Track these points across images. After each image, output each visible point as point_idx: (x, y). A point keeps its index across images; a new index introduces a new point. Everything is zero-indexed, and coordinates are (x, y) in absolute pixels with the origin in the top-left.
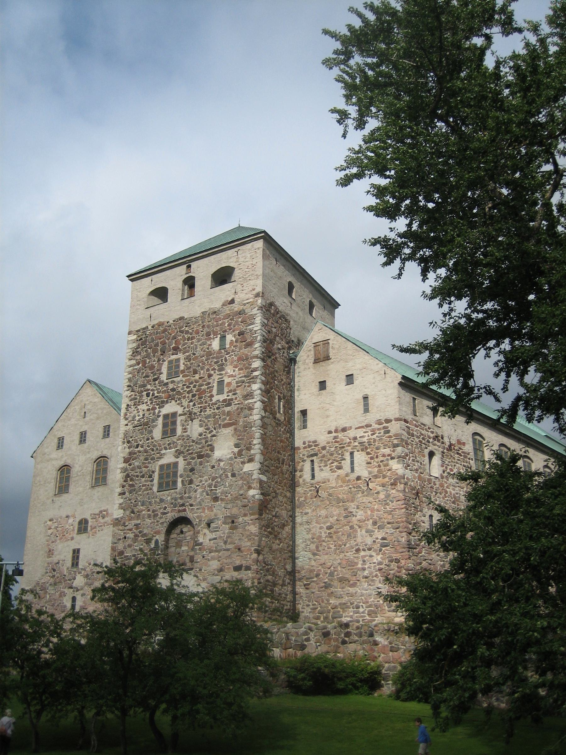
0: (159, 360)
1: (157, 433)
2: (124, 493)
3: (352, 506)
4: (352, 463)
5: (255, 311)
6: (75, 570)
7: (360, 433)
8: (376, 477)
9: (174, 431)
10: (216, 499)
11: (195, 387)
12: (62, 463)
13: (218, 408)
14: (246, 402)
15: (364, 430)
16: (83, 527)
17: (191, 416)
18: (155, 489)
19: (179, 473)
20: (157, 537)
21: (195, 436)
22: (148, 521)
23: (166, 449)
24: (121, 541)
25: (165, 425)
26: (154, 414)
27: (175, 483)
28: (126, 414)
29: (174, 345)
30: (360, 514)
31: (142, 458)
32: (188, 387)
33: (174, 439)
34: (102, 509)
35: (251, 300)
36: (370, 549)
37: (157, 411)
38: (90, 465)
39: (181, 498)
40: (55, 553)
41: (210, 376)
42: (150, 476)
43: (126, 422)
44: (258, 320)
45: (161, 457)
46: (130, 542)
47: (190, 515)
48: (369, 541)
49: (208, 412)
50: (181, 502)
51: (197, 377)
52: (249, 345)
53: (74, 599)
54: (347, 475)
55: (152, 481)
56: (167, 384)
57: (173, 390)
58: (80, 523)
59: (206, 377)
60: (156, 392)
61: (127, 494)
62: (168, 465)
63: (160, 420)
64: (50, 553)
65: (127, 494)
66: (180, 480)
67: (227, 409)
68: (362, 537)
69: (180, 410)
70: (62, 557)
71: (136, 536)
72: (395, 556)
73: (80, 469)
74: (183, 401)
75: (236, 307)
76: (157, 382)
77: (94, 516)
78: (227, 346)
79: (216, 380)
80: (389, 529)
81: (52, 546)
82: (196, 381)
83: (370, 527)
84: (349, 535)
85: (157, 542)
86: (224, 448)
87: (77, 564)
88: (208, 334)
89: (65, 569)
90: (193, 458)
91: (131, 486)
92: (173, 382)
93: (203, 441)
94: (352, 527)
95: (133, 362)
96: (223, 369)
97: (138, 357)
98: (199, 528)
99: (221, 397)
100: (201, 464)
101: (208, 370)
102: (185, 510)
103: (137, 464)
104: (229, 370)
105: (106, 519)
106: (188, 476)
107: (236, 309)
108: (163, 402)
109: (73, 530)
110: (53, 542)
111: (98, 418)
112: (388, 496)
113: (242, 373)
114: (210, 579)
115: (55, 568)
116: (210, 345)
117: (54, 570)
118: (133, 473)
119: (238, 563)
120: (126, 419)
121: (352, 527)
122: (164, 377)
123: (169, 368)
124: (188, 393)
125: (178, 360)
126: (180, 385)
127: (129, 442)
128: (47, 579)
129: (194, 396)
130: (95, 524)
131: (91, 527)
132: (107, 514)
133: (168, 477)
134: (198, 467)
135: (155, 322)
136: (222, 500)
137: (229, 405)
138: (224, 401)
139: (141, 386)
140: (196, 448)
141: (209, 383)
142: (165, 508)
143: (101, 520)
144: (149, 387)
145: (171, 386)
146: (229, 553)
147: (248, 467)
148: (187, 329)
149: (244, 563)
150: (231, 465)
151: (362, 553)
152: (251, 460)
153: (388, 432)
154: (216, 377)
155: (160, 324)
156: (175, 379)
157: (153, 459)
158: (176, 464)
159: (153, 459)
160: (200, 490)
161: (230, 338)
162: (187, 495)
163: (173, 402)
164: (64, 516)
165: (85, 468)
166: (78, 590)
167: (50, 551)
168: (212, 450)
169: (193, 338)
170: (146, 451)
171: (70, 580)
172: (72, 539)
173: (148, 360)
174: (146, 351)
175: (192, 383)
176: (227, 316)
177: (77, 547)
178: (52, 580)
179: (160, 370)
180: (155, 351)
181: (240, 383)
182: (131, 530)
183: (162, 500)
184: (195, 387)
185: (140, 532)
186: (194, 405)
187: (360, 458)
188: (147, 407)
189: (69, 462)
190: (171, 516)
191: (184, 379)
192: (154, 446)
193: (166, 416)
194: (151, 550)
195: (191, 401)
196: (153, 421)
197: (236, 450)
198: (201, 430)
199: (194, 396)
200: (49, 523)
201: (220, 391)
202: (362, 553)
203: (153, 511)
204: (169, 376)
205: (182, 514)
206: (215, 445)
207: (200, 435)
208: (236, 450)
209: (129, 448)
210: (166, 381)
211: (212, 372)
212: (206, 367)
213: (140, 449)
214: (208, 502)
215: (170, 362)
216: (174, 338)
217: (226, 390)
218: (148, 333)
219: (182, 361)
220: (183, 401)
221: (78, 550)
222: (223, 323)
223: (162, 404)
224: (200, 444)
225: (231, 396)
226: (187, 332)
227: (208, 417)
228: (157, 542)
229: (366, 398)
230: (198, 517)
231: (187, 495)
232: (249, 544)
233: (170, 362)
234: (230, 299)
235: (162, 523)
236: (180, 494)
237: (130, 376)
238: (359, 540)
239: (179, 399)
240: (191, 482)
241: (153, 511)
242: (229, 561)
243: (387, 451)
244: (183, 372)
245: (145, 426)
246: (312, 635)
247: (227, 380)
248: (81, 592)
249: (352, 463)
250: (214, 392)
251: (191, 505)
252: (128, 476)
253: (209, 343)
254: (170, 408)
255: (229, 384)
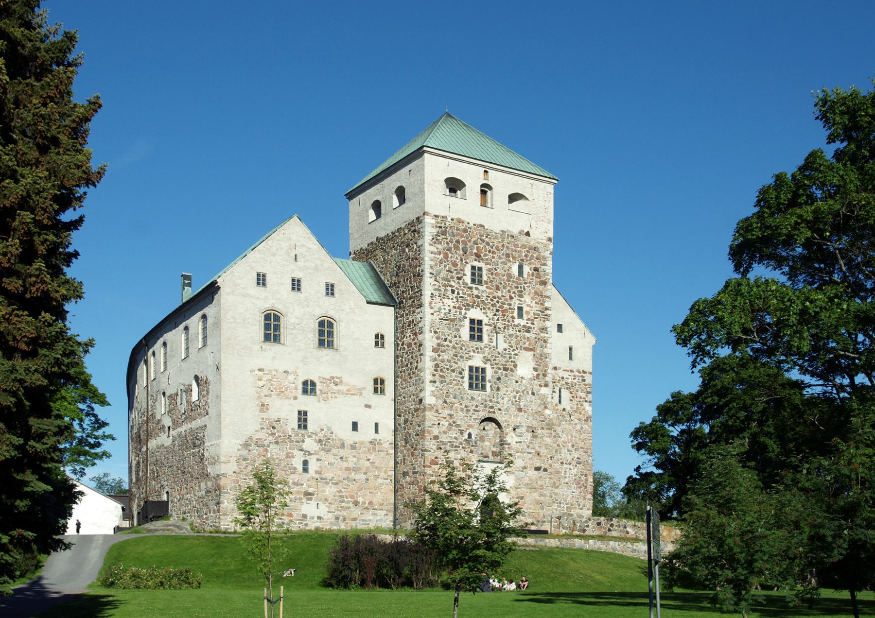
0: (461, 260)
1: (465, 332)
2: (435, 382)
3: (559, 430)
4: (560, 397)
5: (547, 254)
6: (303, 432)
7: (566, 375)
8: (575, 411)
9: (480, 339)
10: (520, 410)
11: (498, 302)
12: (268, 305)
13: (519, 331)
14: (542, 335)
15: (570, 373)
16: (309, 388)
17: (496, 330)
18: (466, 385)
19: (487, 379)
20: (471, 430)
21: (500, 349)
22: (461, 414)
23: (474, 352)
24: (436, 426)
25: (472, 329)
26: (460, 313)
27: (484, 388)
28: (431, 303)
29: (475, 251)
30: (564, 438)
31: (452, 353)
32: (491, 300)
33: (482, 345)
34: (334, 375)
35: (544, 242)
36: (570, 464)
37: (463, 311)
38: (312, 321)
39: (491, 401)
40: (271, 409)
41: (511, 298)
42: (461, 373)
43: (432, 311)
44: (550, 263)
45: (469, 358)
46: (444, 429)
47: (499, 419)
48: (569, 458)
49: (511, 331)
50: (491, 404)
51: (499, 294)
52: (544, 283)
53: (305, 463)
54: (556, 405)
55: (463, 378)
56: (471, 288)
57: (478, 297)
58: (305, 383)
59: (508, 297)
60: (461, 292)
61: (438, 383)
62: (477, 369)
63: (467, 323)
64: (264, 407)
65: (438, 383)
66: (488, 385)
67: (527, 335)
68: (565, 455)
69: (485, 321)
70: (282, 416)
71: (450, 424)
72: (585, 472)
73: (297, 321)
74: (489, 312)
75: (532, 241)
76: (461, 282)
77: (324, 380)
78: (525, 276)
79: (517, 305)
80: (581, 451)
81: (266, 400)
82: (499, 298)
83: (570, 448)
84: (556, 451)
85: (470, 435)
86: (525, 368)
87: (305, 427)
88: (508, 255)
89: (290, 430)
90: (500, 369)
91: (440, 376)
92: (477, 289)
93: (508, 356)
94: (558, 445)
95: (434, 249)
96: (521, 296)
97: (439, 246)
98: (507, 430)
99: (523, 322)
100: (506, 376)
101: (509, 291)
102: (494, 412)
103: (446, 357)
104: (527, 299)
105: (340, 387)
106: (495, 383)
107: (532, 243)
108: (468, 305)
109: (296, 389)
110: (266, 396)
111: (316, 269)
112: (582, 428)
113: (539, 307)
114: (517, 473)
115: (275, 424)
116: (510, 268)
117: (274, 428)
118: (442, 364)
119: (538, 465)
120: (432, 308)
121: (558, 445)
122: (468, 279)
123: (473, 274)
124: (493, 305)
125: (480, 269)
126: (485, 295)
127: (436, 332)
128: (262, 435)
129: (497, 311)
130: (325, 389)
131: (321, 390)
132: (341, 382)
133: (477, 378)
134: (503, 378)
135: (455, 217)
136: (525, 412)
137: (528, 331)
138: (524, 326)
139: (443, 279)
140: (502, 361)
141: (510, 305)
142: (477, 406)
143: (332, 385)
144: (453, 283)
145: (475, 292)
146: (530, 456)
147: (544, 391)
148: (487, 240)
149: (543, 466)
150: (531, 385)
151: (565, 466)
152: (546, 385)
153: (584, 380)
154: (515, 303)
155: (460, 221)
156: (479, 287)
157: (462, 357)
158: (484, 370)
159: (462, 357)
160: (506, 399)
161: (526, 269)
162: (495, 400)
163: (479, 309)
164: (281, 370)
165: (305, 322)
166: (310, 454)
167: (263, 405)
168: (515, 366)
169: (493, 253)
170: (455, 348)
171: (298, 442)
172: (295, 398)
173: (450, 255)
174: (447, 243)
175: (495, 297)
176: (524, 246)
177: (303, 408)
178: (271, 438)
179: (462, 270)
180: (457, 248)
181: (536, 316)
182: (445, 418)
183: (473, 398)
184: (498, 302)
185: (454, 422)
186: (498, 320)
187: (565, 394)
188: (453, 305)
189: (279, 307)
190: (483, 414)
191: (488, 291)
192: (463, 345)
193: (472, 321)
194: (466, 440)
195: (495, 315)
196: (460, 320)
197: (535, 373)
198: (506, 346)
199: (497, 311)
200: (257, 372)
201: (520, 316)
202: (565, 466)
203: (466, 406)
204: (473, 281)
205: (492, 416)
206: (517, 363)
207: (505, 350)
208: (535, 373)
209: (437, 338)
210: (470, 285)
211: (513, 295)
212: (509, 288)
213: (447, 343)
214: (513, 409)
215: (473, 268)
216: (475, 243)
217: (525, 316)
218: (447, 224)
219: (484, 272)
220: (489, 312)
221: (305, 413)
222: (520, 252)
223: (468, 307)
224: (505, 357)
225: (529, 325)
226: (488, 244)
227: (511, 336)
228: (470, 435)
229: (571, 349)
230: (506, 421)
231: (495, 400)
232: (546, 451)
233: (473, 268)
234: (526, 231)
235: (475, 419)
236: (489, 397)
237: (432, 263)
238: (563, 455)
239: (484, 309)
240: (498, 389)
241: (466, 406)
242: (531, 462)
243: (583, 395)
244: (486, 283)
245: (451, 321)
246: (590, 523)
247: (525, 309)
248: (316, 457)
249: (560, 397)
250: (516, 314)
251: (500, 410)
252: (437, 365)
253: (509, 264)
254: (475, 313)
255: (528, 313)
